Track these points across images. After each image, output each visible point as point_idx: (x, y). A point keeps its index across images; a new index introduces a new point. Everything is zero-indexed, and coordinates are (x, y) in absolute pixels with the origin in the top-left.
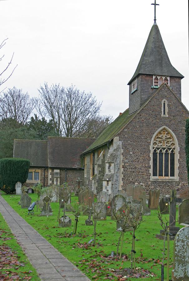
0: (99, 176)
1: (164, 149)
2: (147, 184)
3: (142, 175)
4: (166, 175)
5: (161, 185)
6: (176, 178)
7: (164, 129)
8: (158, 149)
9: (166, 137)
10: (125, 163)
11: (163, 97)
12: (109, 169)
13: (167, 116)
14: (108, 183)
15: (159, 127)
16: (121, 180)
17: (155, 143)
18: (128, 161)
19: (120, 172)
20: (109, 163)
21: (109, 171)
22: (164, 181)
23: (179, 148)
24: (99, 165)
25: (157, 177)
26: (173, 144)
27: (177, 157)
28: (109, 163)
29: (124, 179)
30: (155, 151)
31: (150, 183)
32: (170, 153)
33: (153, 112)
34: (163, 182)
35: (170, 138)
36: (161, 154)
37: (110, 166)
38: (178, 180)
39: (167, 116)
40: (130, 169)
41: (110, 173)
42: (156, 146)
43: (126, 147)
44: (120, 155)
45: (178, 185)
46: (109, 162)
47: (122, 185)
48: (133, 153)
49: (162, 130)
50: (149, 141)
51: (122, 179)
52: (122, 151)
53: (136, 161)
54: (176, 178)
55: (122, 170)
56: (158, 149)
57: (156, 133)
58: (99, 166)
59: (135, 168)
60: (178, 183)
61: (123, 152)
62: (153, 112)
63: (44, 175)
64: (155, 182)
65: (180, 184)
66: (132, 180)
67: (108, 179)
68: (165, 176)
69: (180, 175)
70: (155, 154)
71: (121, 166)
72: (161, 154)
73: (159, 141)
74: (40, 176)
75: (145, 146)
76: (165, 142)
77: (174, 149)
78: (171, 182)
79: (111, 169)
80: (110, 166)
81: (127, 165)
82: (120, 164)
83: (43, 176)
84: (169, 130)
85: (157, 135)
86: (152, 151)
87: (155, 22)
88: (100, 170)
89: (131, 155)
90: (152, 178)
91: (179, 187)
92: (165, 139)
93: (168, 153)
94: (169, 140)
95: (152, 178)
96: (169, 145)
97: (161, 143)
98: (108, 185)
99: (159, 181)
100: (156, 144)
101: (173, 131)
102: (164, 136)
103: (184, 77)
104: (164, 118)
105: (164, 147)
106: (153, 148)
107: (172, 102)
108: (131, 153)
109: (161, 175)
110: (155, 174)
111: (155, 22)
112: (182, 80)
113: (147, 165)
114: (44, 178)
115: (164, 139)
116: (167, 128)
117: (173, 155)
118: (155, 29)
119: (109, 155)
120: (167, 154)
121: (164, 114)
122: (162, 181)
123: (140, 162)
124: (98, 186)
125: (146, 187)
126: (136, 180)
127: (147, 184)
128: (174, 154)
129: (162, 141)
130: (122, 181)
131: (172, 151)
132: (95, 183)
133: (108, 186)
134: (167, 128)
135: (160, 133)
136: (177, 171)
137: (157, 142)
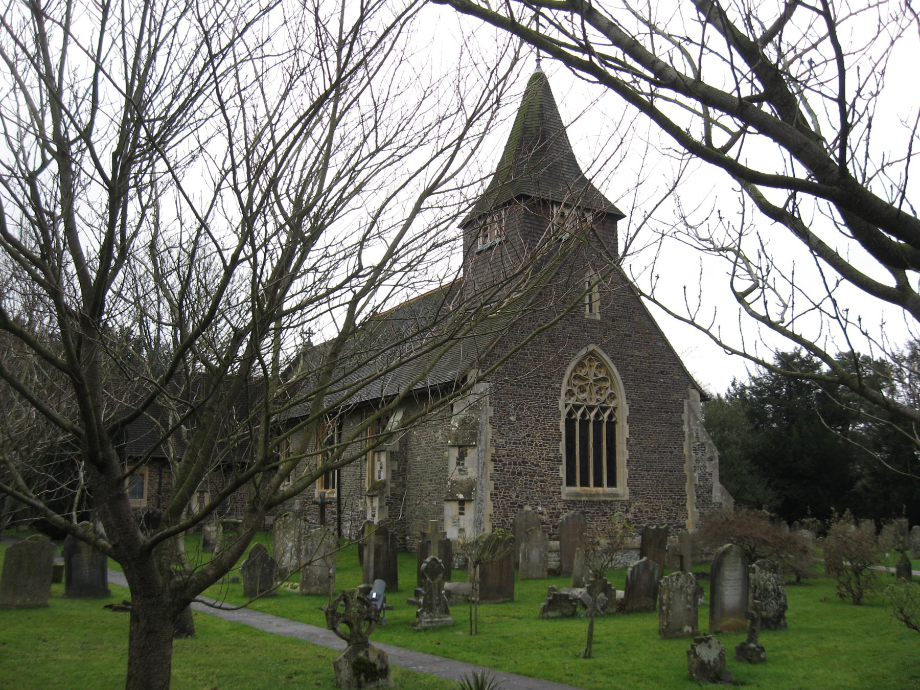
0: (393, 485)
1: (591, 408)
2: (554, 509)
3: (542, 481)
4: (598, 483)
6: (622, 489)
7: (592, 353)
8: (577, 408)
9: (595, 375)
10: (497, 447)
12: (458, 464)
13: (598, 317)
14: (462, 509)
15: (579, 348)
16: (489, 497)
17: (569, 390)
18: (506, 443)
20: (460, 447)
21: (460, 470)
22: (595, 499)
23: (627, 407)
24: (392, 453)
25: (578, 489)
26: (612, 397)
27: (623, 432)
28: (460, 447)
29: (496, 495)
30: (570, 414)
31: (560, 506)
32: (605, 420)
34: (591, 504)
35: (604, 379)
36: (584, 423)
37: (462, 457)
38: (627, 497)
39: (598, 317)
40: (510, 464)
41: (464, 477)
42: (572, 401)
43: (500, 399)
46: (461, 443)
47: (492, 512)
49: (585, 357)
50: (557, 385)
51: (491, 494)
52: (490, 411)
53: (524, 443)
54: (622, 489)
55: (491, 466)
56: (577, 408)
57: (573, 364)
58: (392, 456)
59: (525, 462)
60: (627, 506)
61: (492, 415)
63: (160, 484)
64: (571, 504)
65: (632, 510)
66: (517, 497)
67: (461, 496)
68: (595, 486)
69: (632, 481)
70: (570, 423)
71: (489, 458)
72: (584, 423)
73: (580, 387)
74: (146, 486)
75: (546, 398)
76: (595, 389)
77: (615, 408)
78: (612, 501)
79: (466, 464)
80: (462, 457)
81: (504, 453)
82: (486, 451)
83: (156, 486)
84: (605, 356)
85: (574, 370)
86: (564, 412)
87: (538, 66)
88: (396, 469)
89: (510, 422)
91: (629, 516)
92: (594, 381)
93: (589, 420)
94: (603, 384)
95: (566, 490)
96: (602, 399)
97: (583, 391)
98: (461, 514)
99: (583, 499)
100: (573, 395)
101: (613, 359)
102: (590, 372)
103: (625, 216)
104: (591, 322)
105: (591, 403)
106: (566, 406)
108: (512, 418)
109: (584, 483)
110: (571, 482)
111: (538, 66)
112: (620, 223)
113: (552, 455)
114: (159, 493)
115: (591, 381)
116: (600, 351)
117: (611, 426)
119: (457, 425)
120: (598, 424)
121: (591, 310)
122: (590, 501)
123: (536, 445)
124: (390, 516)
125: (551, 517)
126: (527, 498)
127: (554, 509)
128: (615, 423)
129: (587, 388)
130: (492, 500)
131: (611, 416)
132: (381, 507)
133: (461, 517)
134: (600, 351)
135: (581, 365)
136: (622, 473)
137: (575, 390)
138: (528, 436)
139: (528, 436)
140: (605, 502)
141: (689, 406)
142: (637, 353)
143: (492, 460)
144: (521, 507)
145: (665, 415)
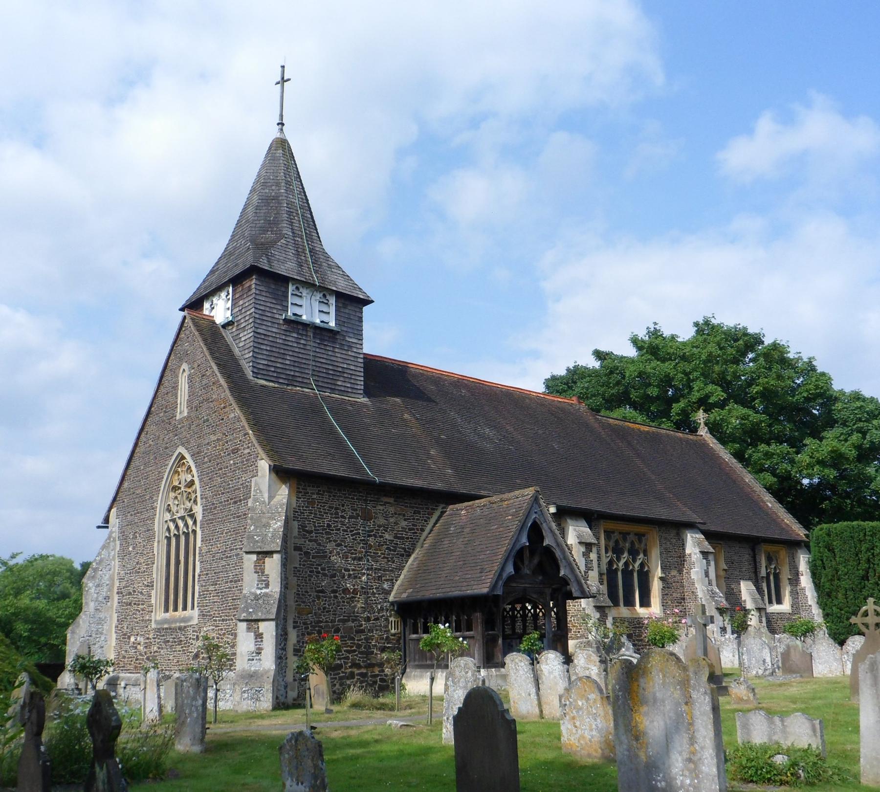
5: (168, 641)
11: (181, 360)
19: (112, 607)
22: (173, 626)
25: (171, 614)
33: (165, 412)
44: (114, 559)
45: (197, 636)
48: (134, 548)
55: (116, 598)
59: (134, 591)
62: (165, 412)
71: (116, 591)
78: (185, 627)
90: (159, 615)
99: (166, 626)
107: (196, 365)
118: (281, 151)
125: (146, 647)
138: (137, 563)
139: (137, 563)
140: (180, 628)
141: (256, 484)
142: (213, 438)
143: (118, 593)
144: (129, 638)
145: (233, 508)
